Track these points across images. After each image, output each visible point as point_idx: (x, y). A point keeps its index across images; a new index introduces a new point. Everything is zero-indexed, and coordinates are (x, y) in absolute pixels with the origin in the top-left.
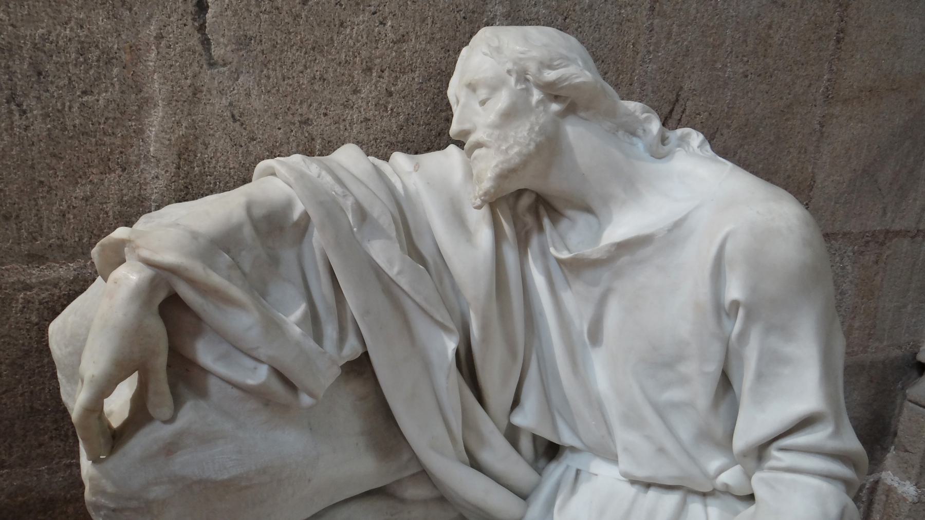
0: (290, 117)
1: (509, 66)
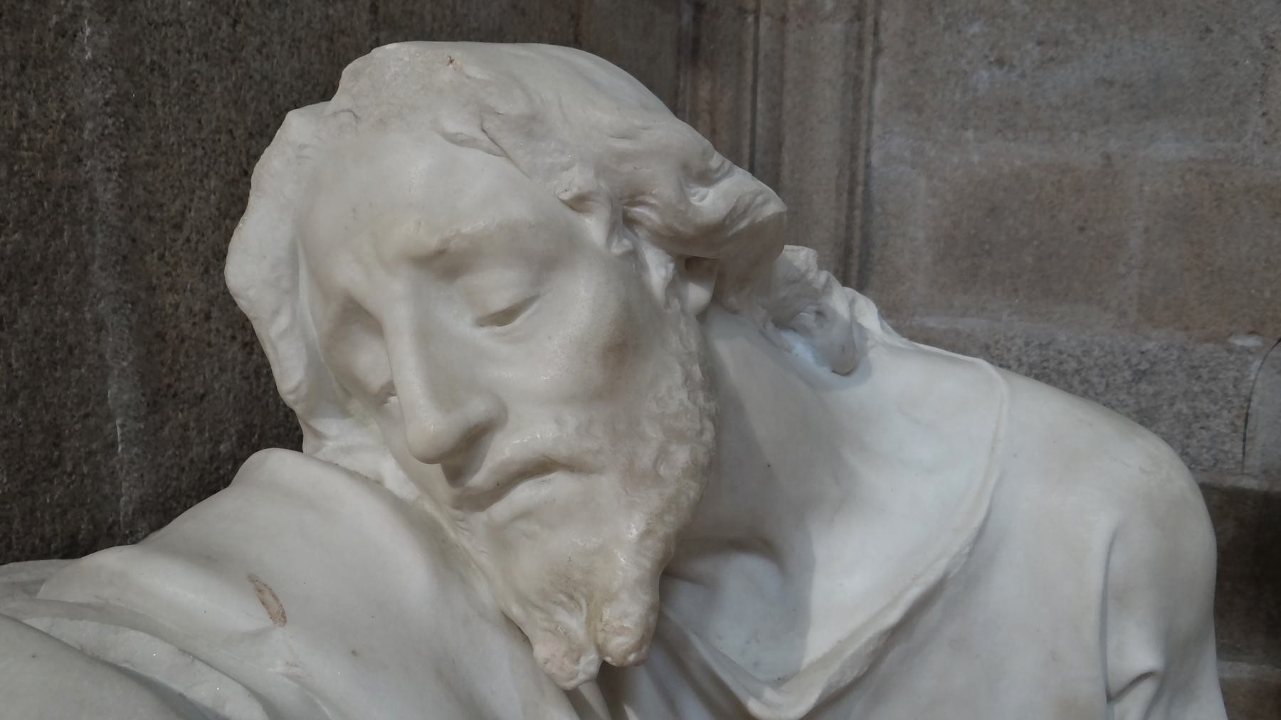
1: (577, 179)
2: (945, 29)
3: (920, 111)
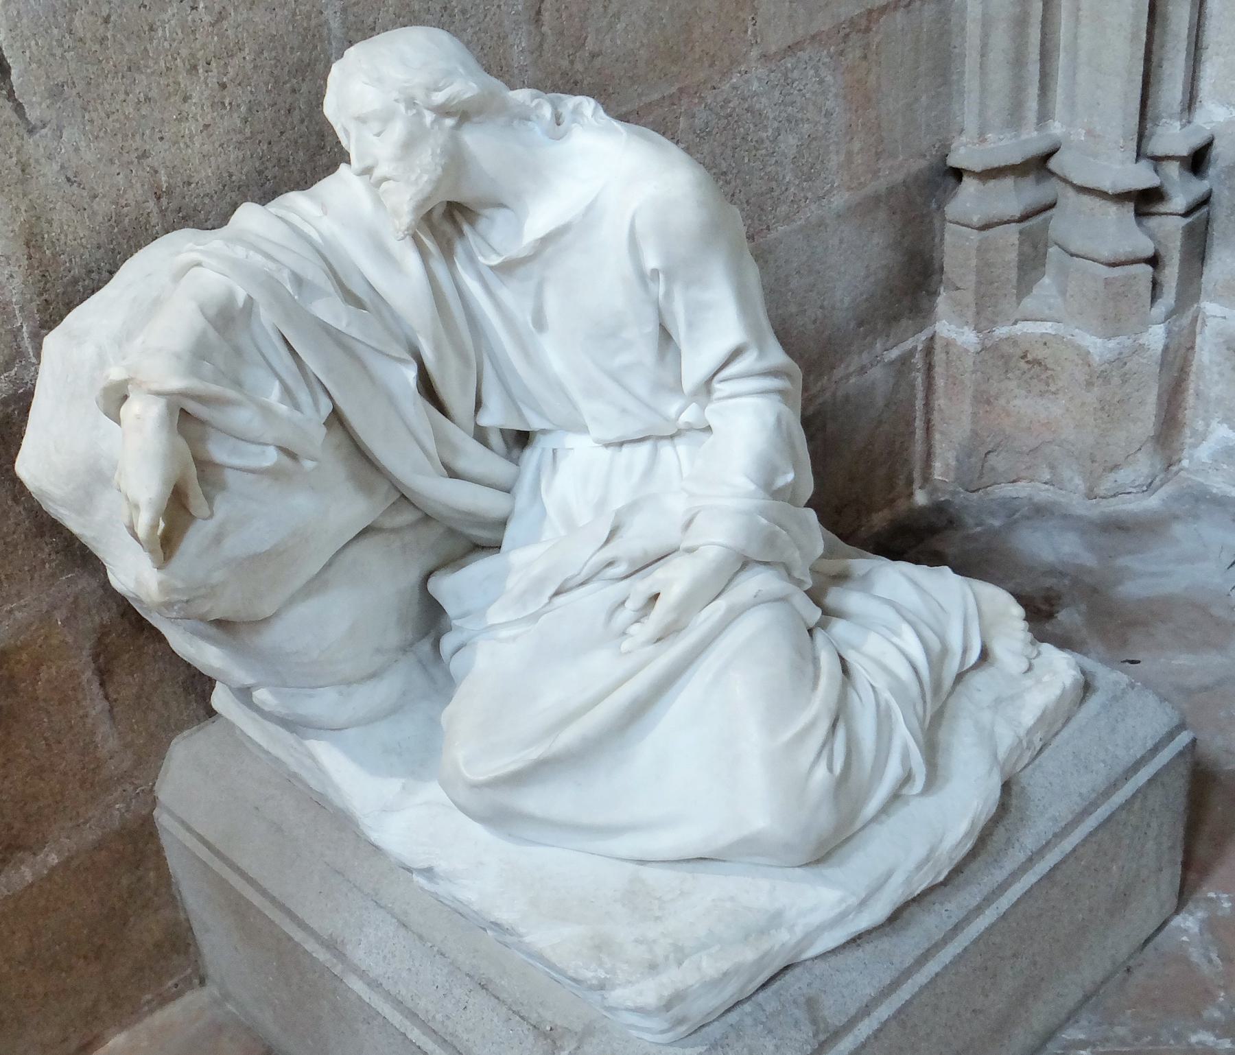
0: (126, 158)
1: (395, 95)
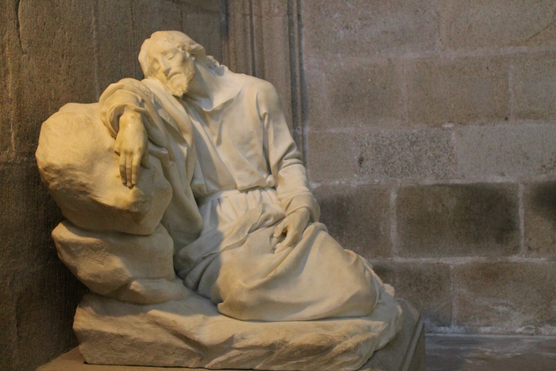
1: (178, 44)
2: (326, 16)
3: (320, 48)
